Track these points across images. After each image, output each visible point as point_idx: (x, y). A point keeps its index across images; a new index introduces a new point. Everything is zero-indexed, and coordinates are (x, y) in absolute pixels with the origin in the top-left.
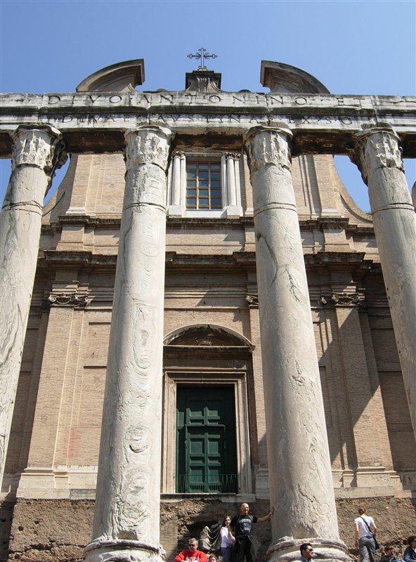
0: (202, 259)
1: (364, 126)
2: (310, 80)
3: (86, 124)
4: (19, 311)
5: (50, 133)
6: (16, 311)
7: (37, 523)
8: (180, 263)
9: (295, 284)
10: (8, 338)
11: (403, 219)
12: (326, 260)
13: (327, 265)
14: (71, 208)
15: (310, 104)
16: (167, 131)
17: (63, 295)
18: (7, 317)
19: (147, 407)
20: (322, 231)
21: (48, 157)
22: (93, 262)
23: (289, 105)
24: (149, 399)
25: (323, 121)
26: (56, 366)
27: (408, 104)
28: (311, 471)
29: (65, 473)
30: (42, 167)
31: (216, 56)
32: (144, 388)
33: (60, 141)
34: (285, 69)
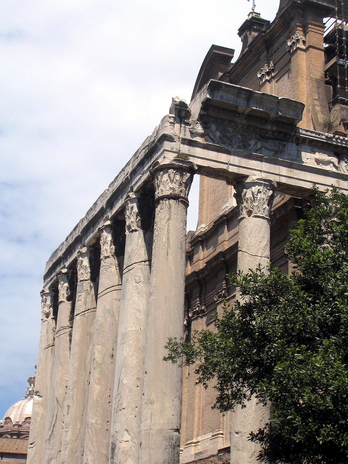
3: (71, 261)
4: (58, 401)
6: (56, 402)
10: (52, 420)
16: (84, 250)
21: (67, 290)
30: (64, 300)
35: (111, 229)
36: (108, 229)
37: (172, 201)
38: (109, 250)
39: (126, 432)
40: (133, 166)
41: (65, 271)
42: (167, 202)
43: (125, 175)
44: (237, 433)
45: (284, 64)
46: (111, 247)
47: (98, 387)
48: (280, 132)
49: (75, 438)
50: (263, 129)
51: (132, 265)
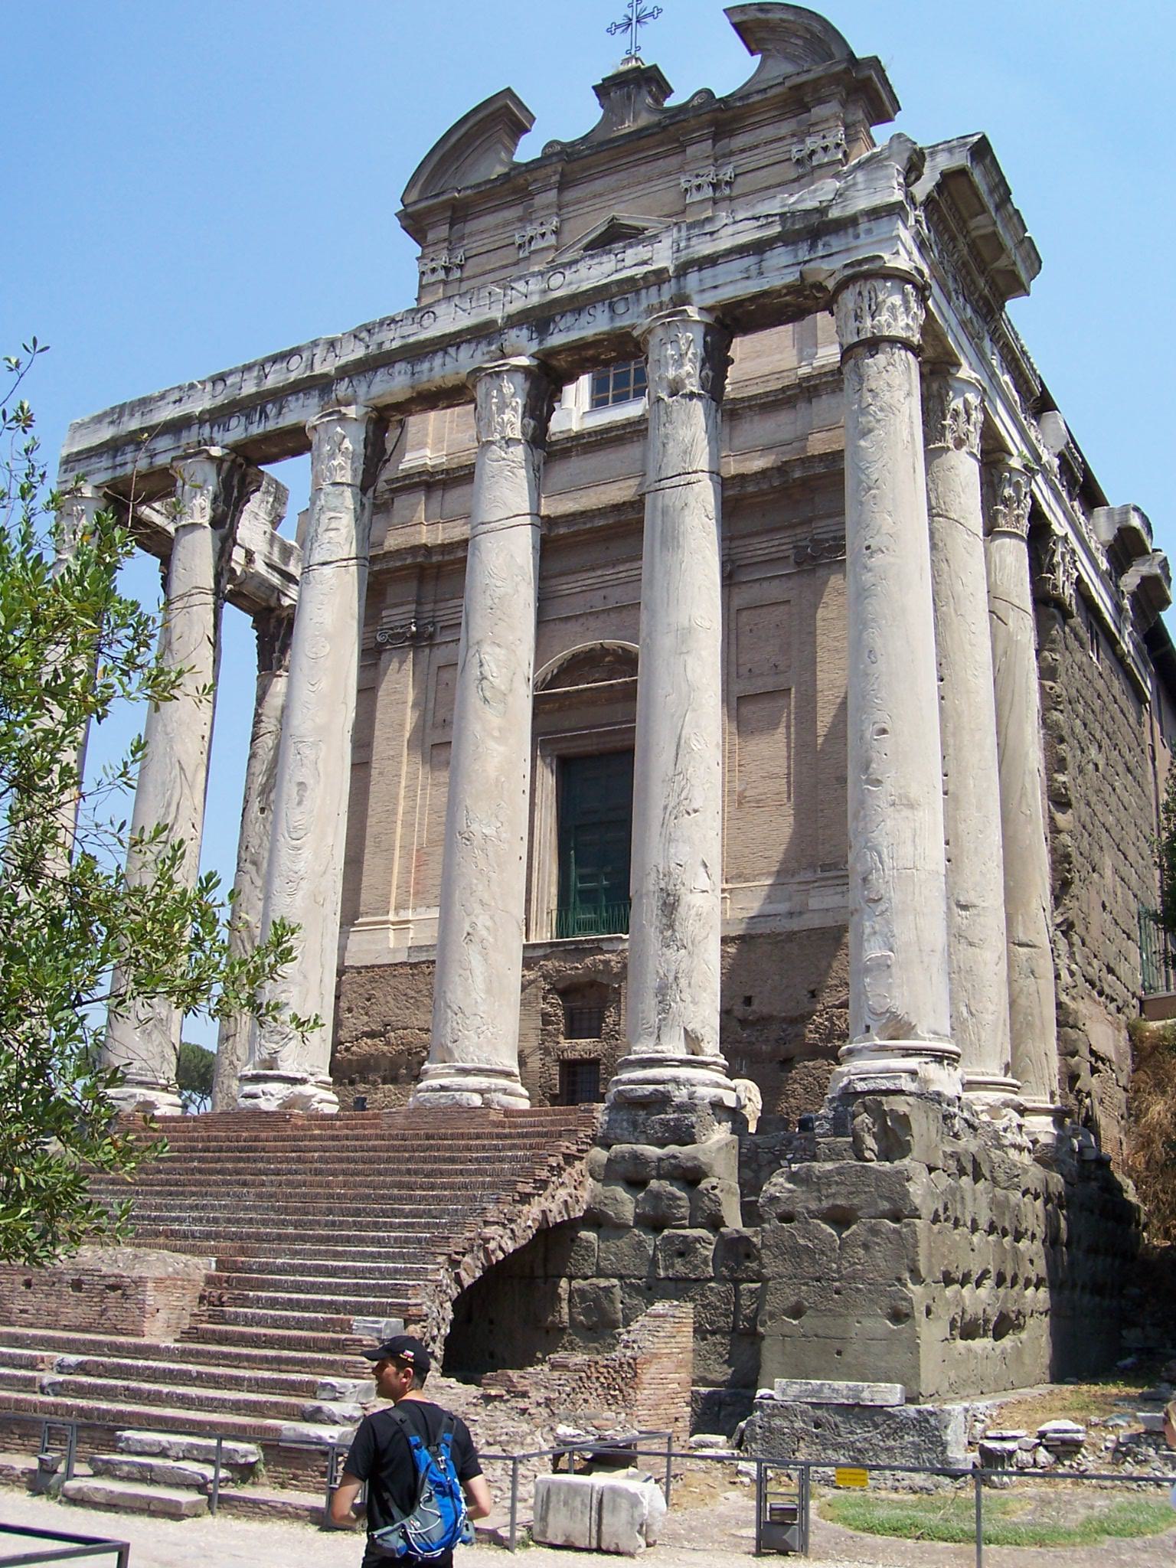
0: (594, 516)
1: (650, 310)
2: (817, 27)
3: (256, 430)
4: (182, 768)
5: (211, 458)
7: (368, 1000)
8: (562, 531)
9: (487, 674)
11: (665, 512)
12: (797, 475)
13: (804, 482)
14: (408, 457)
15: (570, 284)
17: (396, 627)
18: (164, 783)
19: (301, 893)
20: (810, 402)
22: (436, 559)
23: (535, 300)
24: (303, 883)
25: (585, 318)
26: (392, 753)
27: (740, 226)
28: (461, 972)
29: (408, 922)
30: (206, 522)
31: (660, 11)
32: (296, 869)
33: (233, 461)
34: (770, 16)
35: (526, 379)
36: (519, 378)
37: (910, 355)
38: (518, 425)
39: (702, 869)
40: (678, 250)
41: (216, 451)
42: (903, 352)
43: (627, 263)
44: (965, 908)
45: (778, 180)
46: (526, 420)
47: (502, 749)
48: (987, 303)
49: (322, 868)
50: (973, 282)
51: (696, 472)
